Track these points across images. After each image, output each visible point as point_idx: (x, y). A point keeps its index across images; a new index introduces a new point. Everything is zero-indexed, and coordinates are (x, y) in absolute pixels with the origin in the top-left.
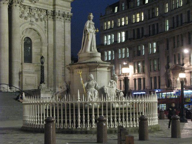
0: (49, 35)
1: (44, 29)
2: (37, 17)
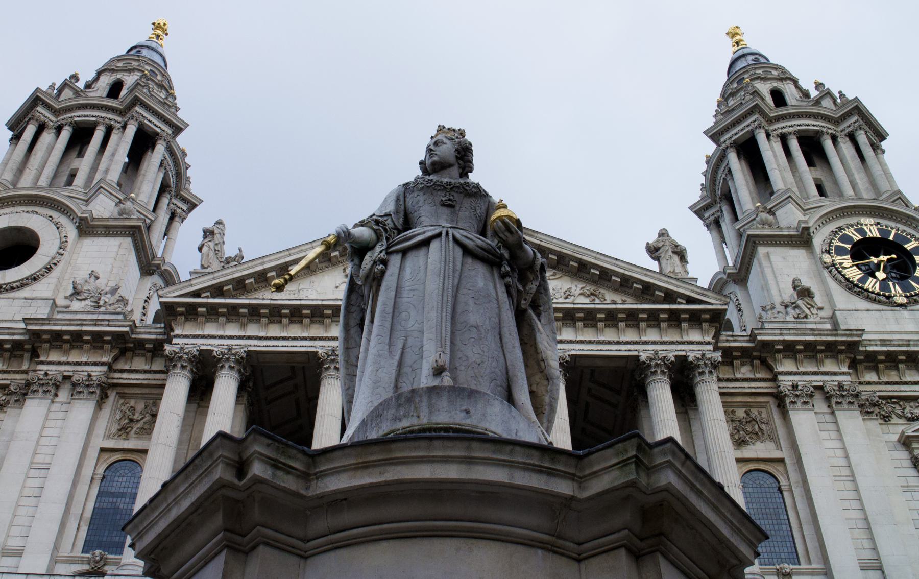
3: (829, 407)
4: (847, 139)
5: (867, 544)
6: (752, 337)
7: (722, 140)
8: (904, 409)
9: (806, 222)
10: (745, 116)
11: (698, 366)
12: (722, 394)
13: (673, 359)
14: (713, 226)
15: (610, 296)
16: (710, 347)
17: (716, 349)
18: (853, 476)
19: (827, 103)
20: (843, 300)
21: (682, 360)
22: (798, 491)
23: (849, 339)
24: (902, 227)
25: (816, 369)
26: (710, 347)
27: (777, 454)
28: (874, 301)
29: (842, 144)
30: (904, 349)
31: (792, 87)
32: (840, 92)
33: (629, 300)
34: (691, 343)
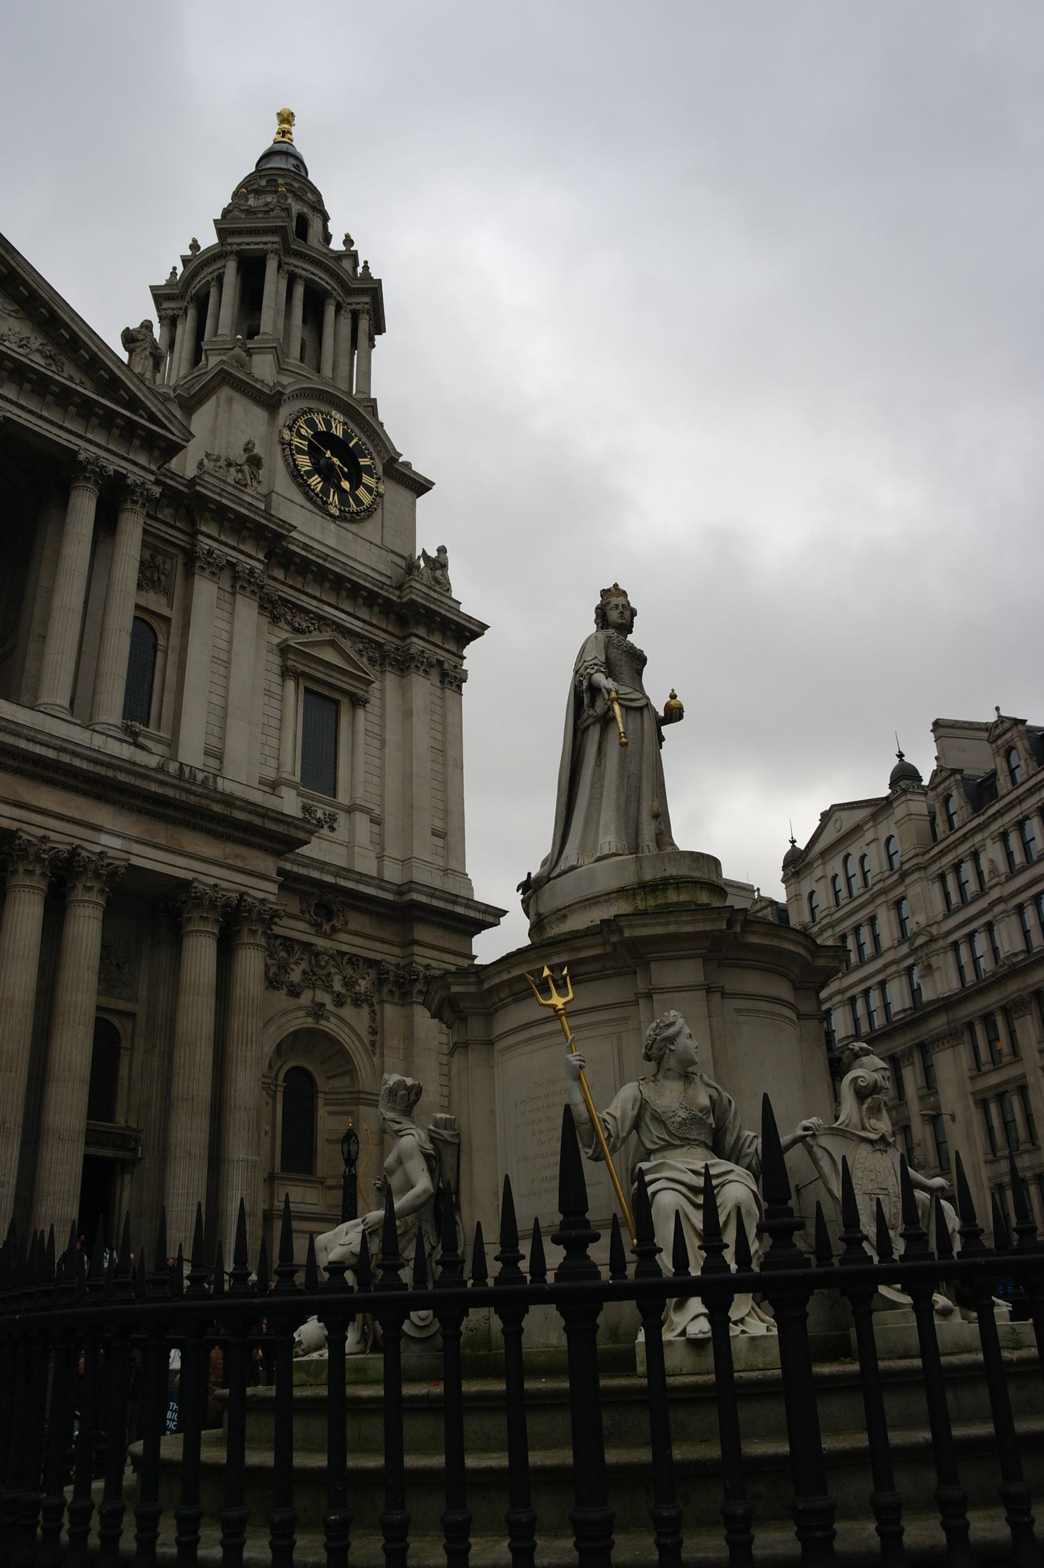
0: (386, 1059)
2: (338, 987)
3: (232, 586)
4: (350, 316)
6: (192, 483)
7: (230, 240)
9: (284, 387)
10: (266, 231)
11: (134, 492)
12: (145, 531)
13: (111, 473)
14: (166, 322)
15: (69, 370)
16: (152, 478)
17: (158, 482)
18: (229, 662)
19: (347, 264)
20: (283, 484)
21: (120, 477)
22: (172, 657)
23: (279, 530)
24: (364, 439)
25: (235, 544)
26: (152, 478)
27: (166, 612)
28: (310, 499)
29: (342, 318)
30: (321, 561)
31: (321, 224)
32: (366, 262)
33: (88, 384)
34: (135, 463)
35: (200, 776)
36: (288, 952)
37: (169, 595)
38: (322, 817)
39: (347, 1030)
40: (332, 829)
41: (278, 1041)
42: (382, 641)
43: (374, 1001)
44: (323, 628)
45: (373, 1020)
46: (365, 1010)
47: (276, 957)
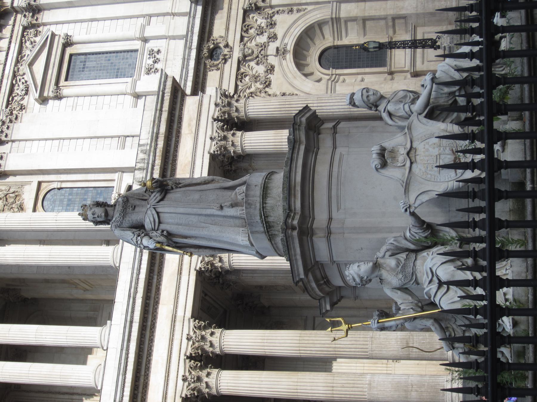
1: (295, 16)
2: (263, 39)
3: (7, 143)
5: (108, 141)
8: (18, 94)
22: (64, 177)
27: (35, 186)
35: (141, 156)
36: (246, 76)
37: (22, 185)
38: (152, 60)
39: (292, 30)
40: (159, 52)
41: (303, 77)
42: (21, 28)
43: (270, 12)
44: (21, 73)
45: (283, 11)
46: (276, 17)
47: (249, 84)
